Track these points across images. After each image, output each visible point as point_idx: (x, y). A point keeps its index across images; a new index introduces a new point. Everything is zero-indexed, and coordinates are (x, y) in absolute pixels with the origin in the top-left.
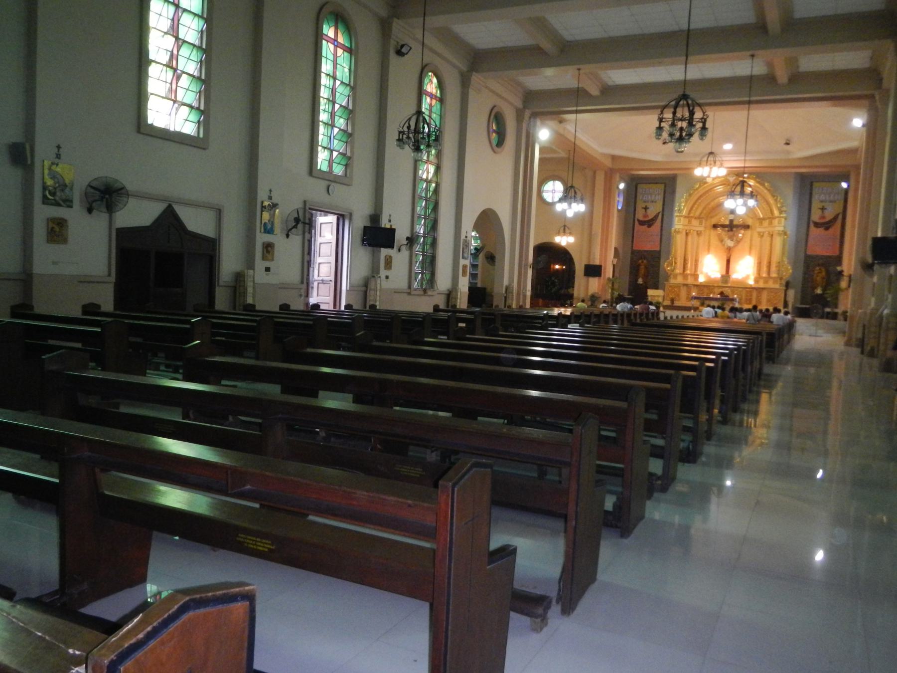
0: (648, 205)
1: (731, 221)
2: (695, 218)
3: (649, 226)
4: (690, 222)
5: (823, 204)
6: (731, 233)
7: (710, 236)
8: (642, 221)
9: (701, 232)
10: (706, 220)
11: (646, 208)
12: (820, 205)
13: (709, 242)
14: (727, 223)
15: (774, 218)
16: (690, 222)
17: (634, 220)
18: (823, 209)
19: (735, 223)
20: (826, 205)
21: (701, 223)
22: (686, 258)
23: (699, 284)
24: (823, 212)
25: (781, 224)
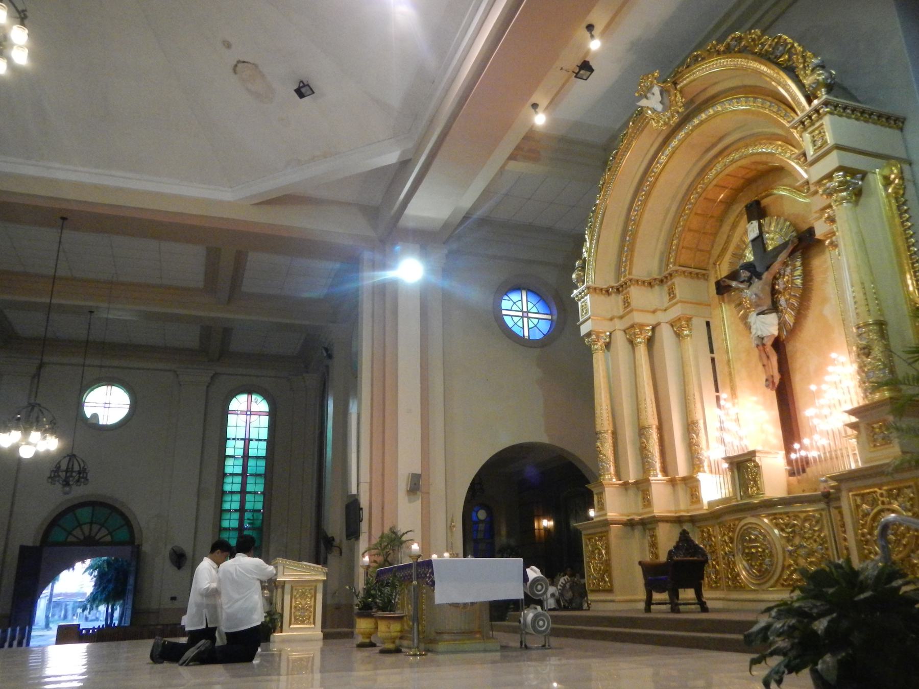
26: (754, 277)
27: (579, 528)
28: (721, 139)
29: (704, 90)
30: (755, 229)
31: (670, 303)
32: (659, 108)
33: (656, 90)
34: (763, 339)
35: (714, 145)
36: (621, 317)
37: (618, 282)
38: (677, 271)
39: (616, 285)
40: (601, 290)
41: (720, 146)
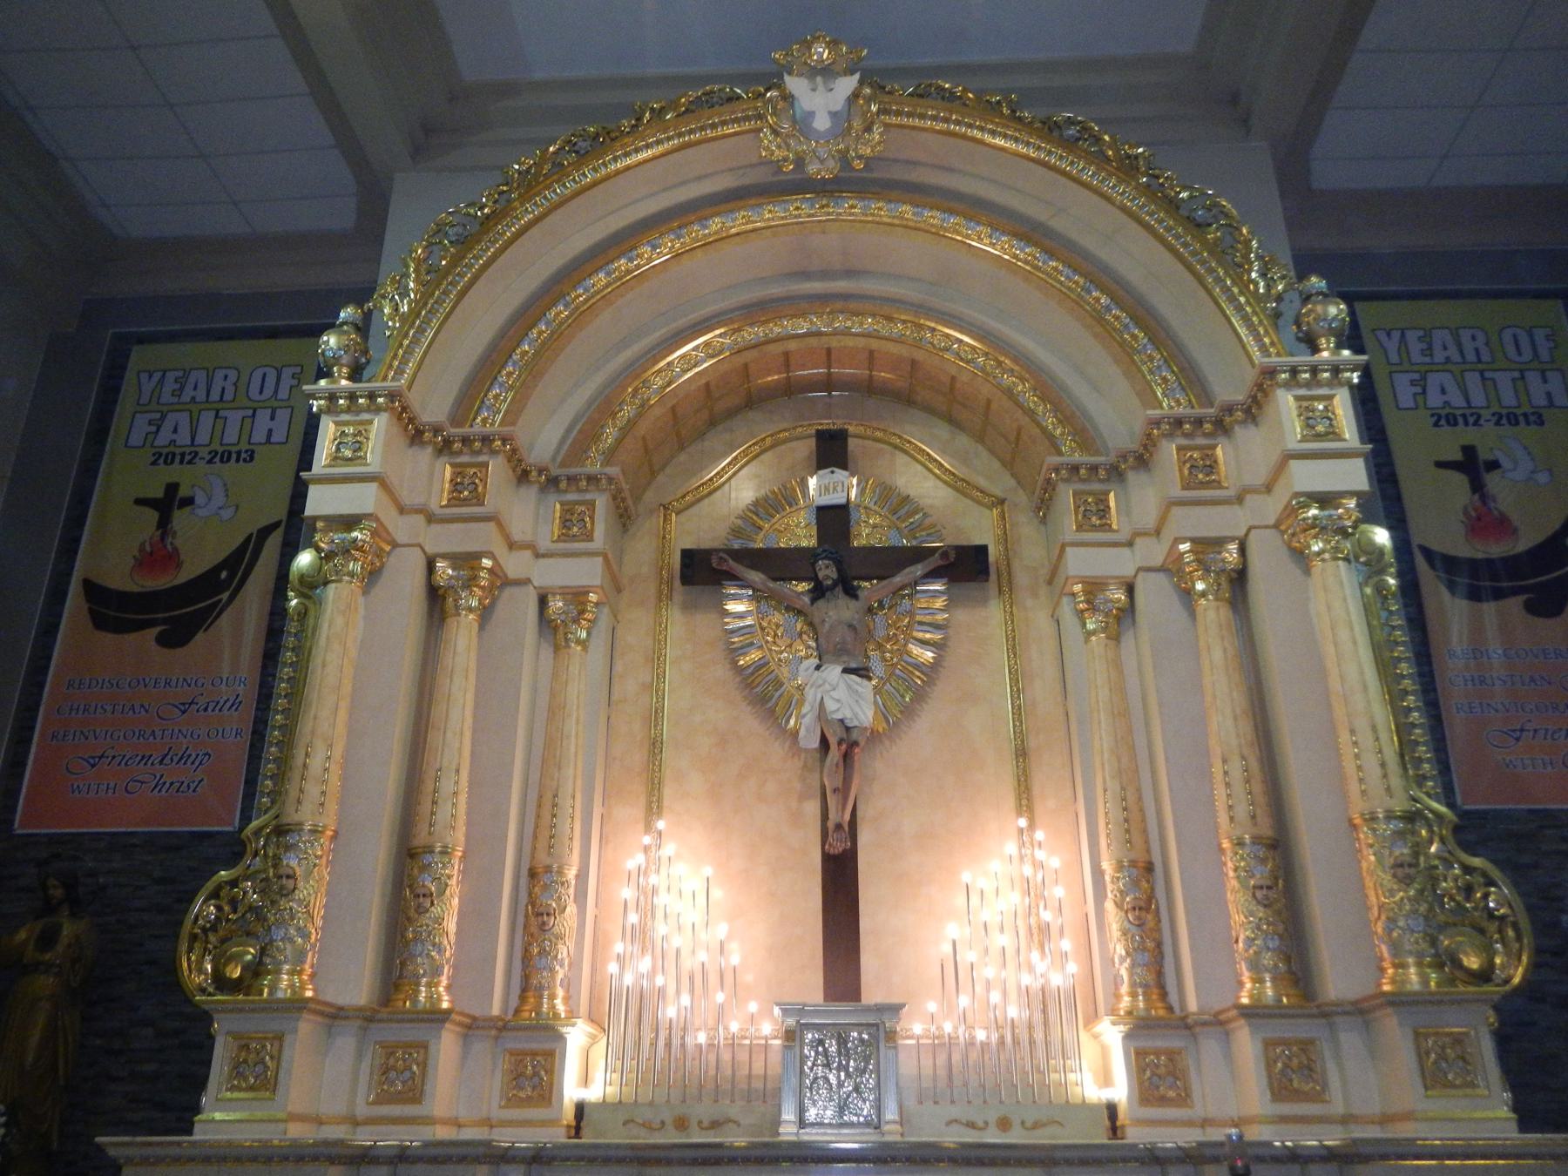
0: (187, 478)
1: (834, 519)
2: (523, 477)
3: (176, 637)
4: (466, 490)
5: (1469, 435)
6: (838, 611)
7: (659, 641)
8: (124, 599)
9: (577, 597)
10: (624, 518)
11: (168, 503)
12: (1450, 444)
13: (655, 716)
14: (800, 532)
15: (1253, 408)
16: (466, 490)
17: (57, 595)
18: (1471, 466)
19: (867, 533)
20: (1487, 441)
21: (573, 525)
22: (421, 838)
23: (557, 1136)
24: (1477, 486)
25: (1333, 434)
26: (839, 589)
27: (112, 1152)
28: (849, 273)
29: (914, 163)
30: (839, 488)
31: (561, 545)
32: (822, 123)
33: (847, 84)
34: (848, 729)
35: (825, 275)
36: (431, 519)
37: (460, 424)
38: (610, 480)
39: (453, 431)
40: (411, 420)
41: (841, 285)
